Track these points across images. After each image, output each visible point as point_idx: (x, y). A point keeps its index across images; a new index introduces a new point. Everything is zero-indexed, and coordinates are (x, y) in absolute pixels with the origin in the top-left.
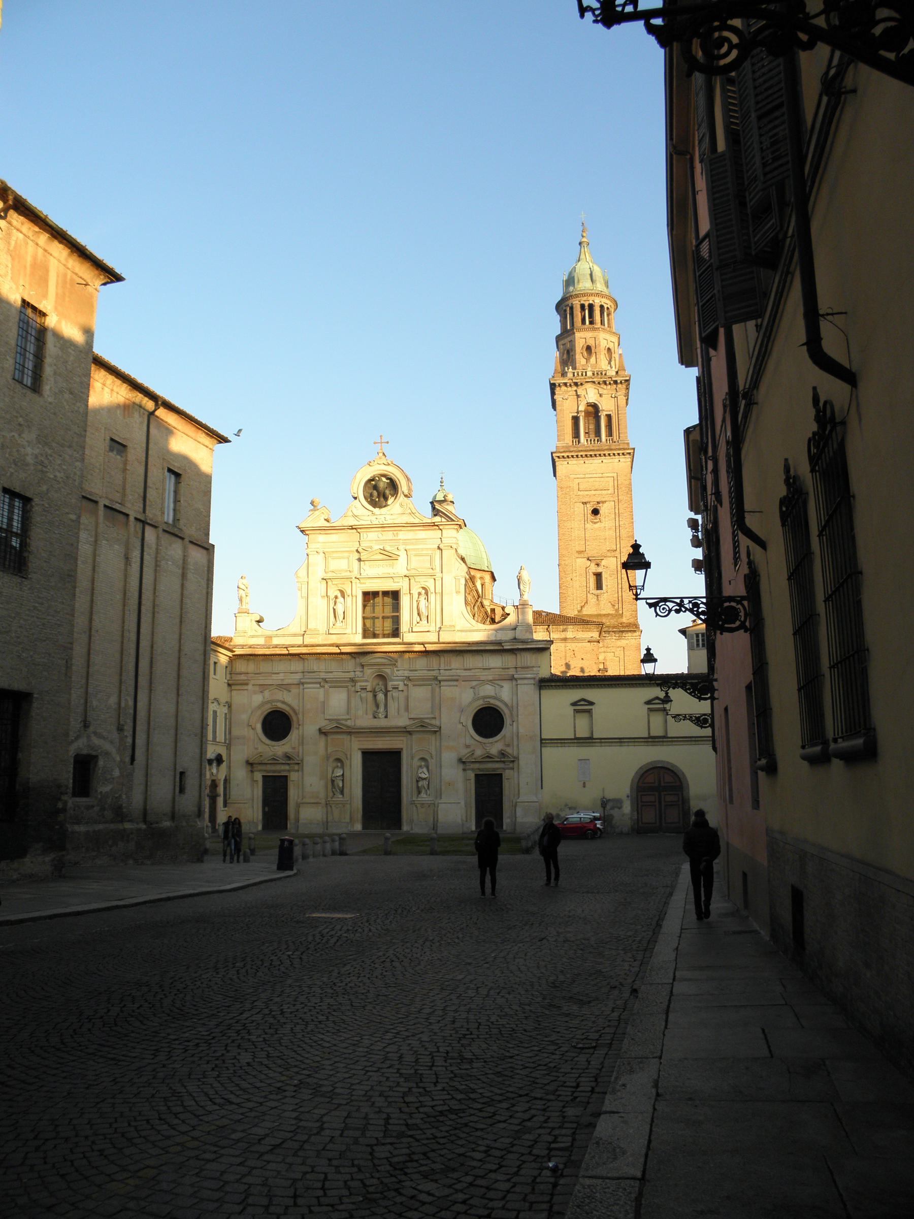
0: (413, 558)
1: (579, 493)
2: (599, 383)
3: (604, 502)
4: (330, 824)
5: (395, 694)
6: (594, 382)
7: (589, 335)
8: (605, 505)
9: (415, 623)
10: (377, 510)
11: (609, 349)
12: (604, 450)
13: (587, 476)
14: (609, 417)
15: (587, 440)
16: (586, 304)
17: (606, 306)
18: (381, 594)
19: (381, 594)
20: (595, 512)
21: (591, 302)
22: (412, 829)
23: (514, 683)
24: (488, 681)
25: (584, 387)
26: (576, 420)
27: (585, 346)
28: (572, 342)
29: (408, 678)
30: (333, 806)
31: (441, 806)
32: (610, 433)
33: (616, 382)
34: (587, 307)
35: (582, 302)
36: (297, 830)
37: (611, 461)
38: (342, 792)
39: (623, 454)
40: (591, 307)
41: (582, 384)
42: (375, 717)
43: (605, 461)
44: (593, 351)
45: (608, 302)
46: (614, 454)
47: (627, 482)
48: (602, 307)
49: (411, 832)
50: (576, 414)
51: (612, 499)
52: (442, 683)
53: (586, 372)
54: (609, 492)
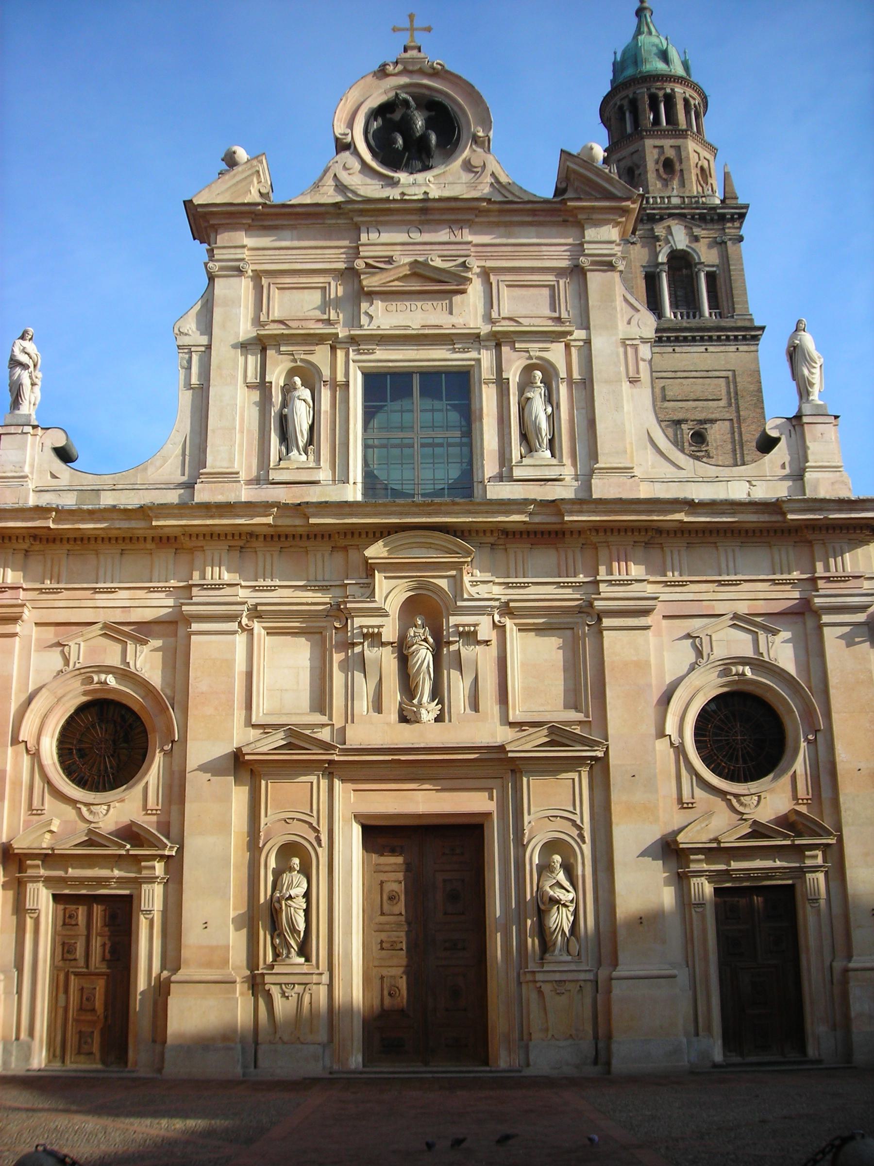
0: (505, 292)
1: (666, 404)
2: (693, 218)
3: (713, 421)
4: (262, 1049)
5: (467, 652)
6: (682, 216)
7: (667, 143)
8: (716, 426)
9: (516, 456)
10: (403, 177)
11: (702, 169)
12: (709, 329)
13: (679, 374)
14: (711, 278)
15: (674, 313)
16: (661, 94)
17: (692, 102)
18: (416, 381)
19: (416, 381)
20: (699, 438)
21: (668, 91)
22: (528, 1065)
23: (810, 623)
24: (736, 616)
25: (666, 223)
26: (652, 280)
27: (662, 159)
28: (640, 153)
29: (507, 609)
30: (275, 991)
31: (618, 990)
32: (714, 303)
33: (722, 218)
34: (662, 99)
35: (653, 90)
36: (160, 1070)
37: (722, 348)
38: (304, 950)
39: (744, 338)
40: (670, 100)
41: (662, 219)
42: (404, 719)
43: (711, 349)
44: (677, 167)
45: (695, 95)
46: (728, 337)
47: (752, 387)
48: (686, 101)
49: (527, 1072)
50: (652, 270)
51: (727, 416)
52: (606, 622)
53: (669, 197)
54: (723, 403)
